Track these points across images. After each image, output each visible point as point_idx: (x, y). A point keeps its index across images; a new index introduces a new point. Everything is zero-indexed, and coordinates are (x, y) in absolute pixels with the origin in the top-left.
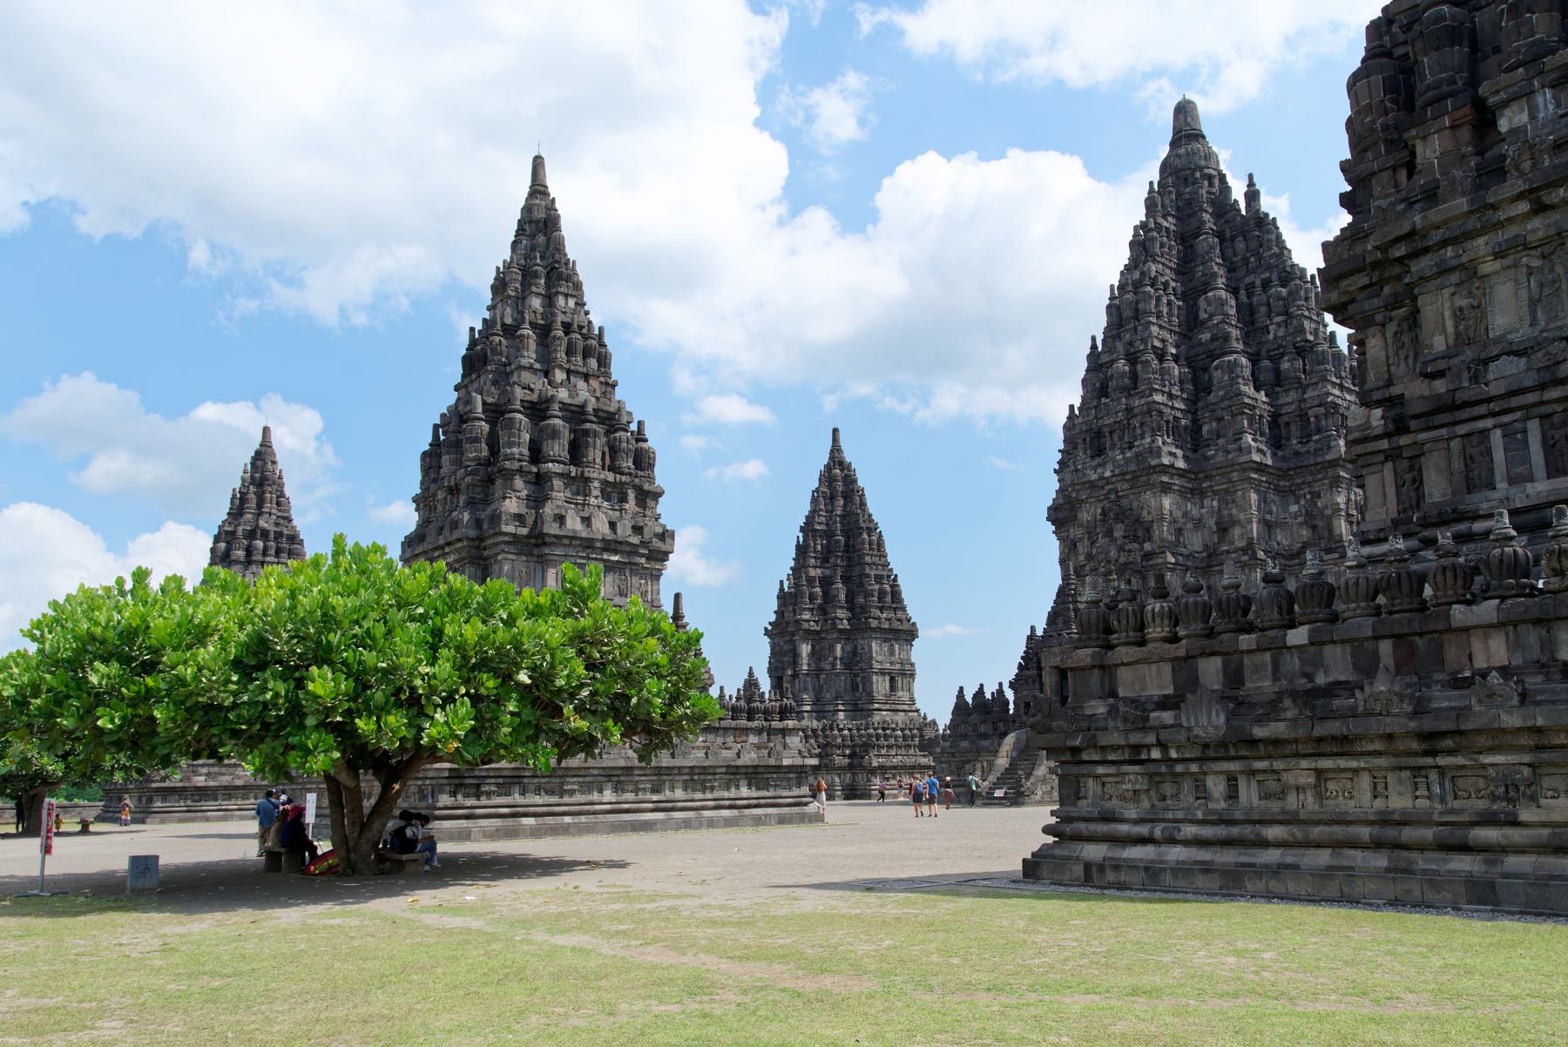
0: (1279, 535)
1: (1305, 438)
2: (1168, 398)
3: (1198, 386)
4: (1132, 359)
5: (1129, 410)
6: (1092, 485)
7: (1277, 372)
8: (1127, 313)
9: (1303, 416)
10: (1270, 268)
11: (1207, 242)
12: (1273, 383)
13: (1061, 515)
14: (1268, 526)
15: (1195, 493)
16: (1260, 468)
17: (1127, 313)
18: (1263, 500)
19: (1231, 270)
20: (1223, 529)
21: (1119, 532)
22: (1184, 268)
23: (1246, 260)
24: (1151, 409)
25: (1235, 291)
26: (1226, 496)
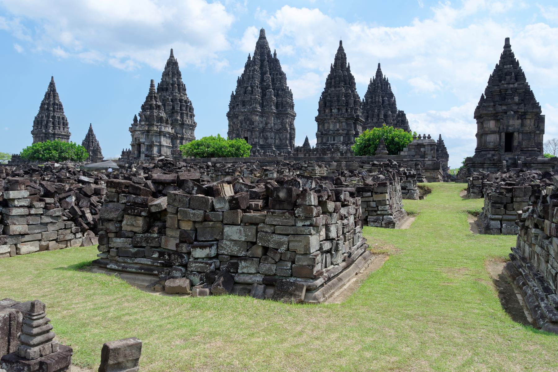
0: (276, 126)
1: (282, 108)
2: (258, 97)
3: (264, 95)
4: (252, 87)
5: (251, 98)
6: (242, 112)
7: (278, 93)
8: (251, 77)
9: (282, 103)
10: (278, 71)
11: (266, 63)
12: (277, 95)
13: (230, 116)
14: (274, 124)
15: (262, 116)
16: (274, 113)
17: (251, 77)
18: (274, 119)
19: (270, 69)
20: (266, 124)
21: (248, 123)
22: (261, 67)
23: (273, 68)
24: (255, 99)
25: (270, 74)
26: (268, 118)
